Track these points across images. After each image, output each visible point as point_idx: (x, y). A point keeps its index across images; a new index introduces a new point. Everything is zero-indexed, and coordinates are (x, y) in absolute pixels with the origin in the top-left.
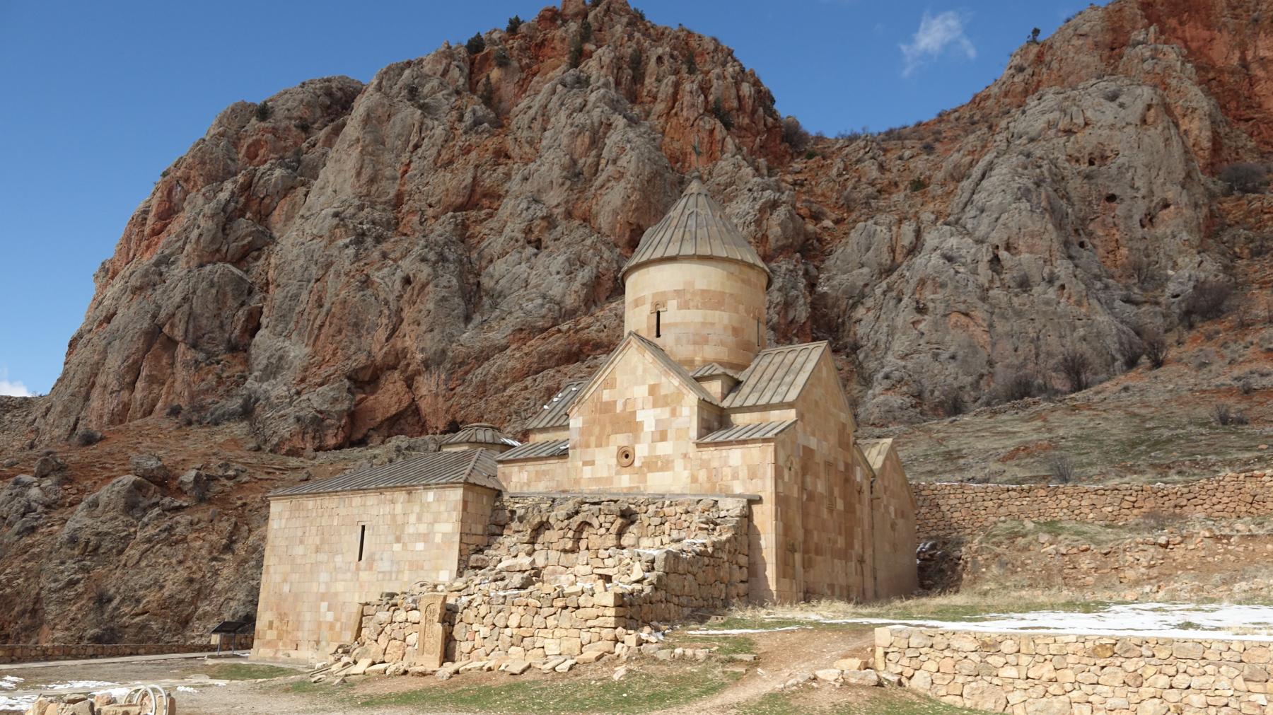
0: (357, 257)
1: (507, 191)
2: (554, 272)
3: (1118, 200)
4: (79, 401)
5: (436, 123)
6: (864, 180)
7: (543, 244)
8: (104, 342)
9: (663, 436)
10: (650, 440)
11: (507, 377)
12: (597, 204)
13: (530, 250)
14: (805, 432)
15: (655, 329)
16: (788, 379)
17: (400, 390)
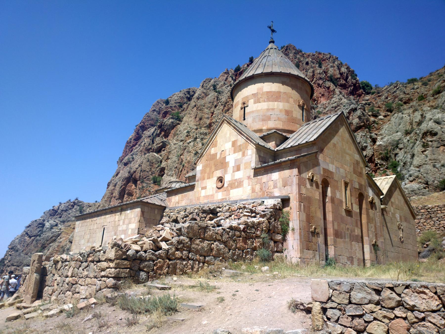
0: (194, 146)
4: (108, 202)
5: (222, 97)
9: (238, 168)
15: (243, 116)
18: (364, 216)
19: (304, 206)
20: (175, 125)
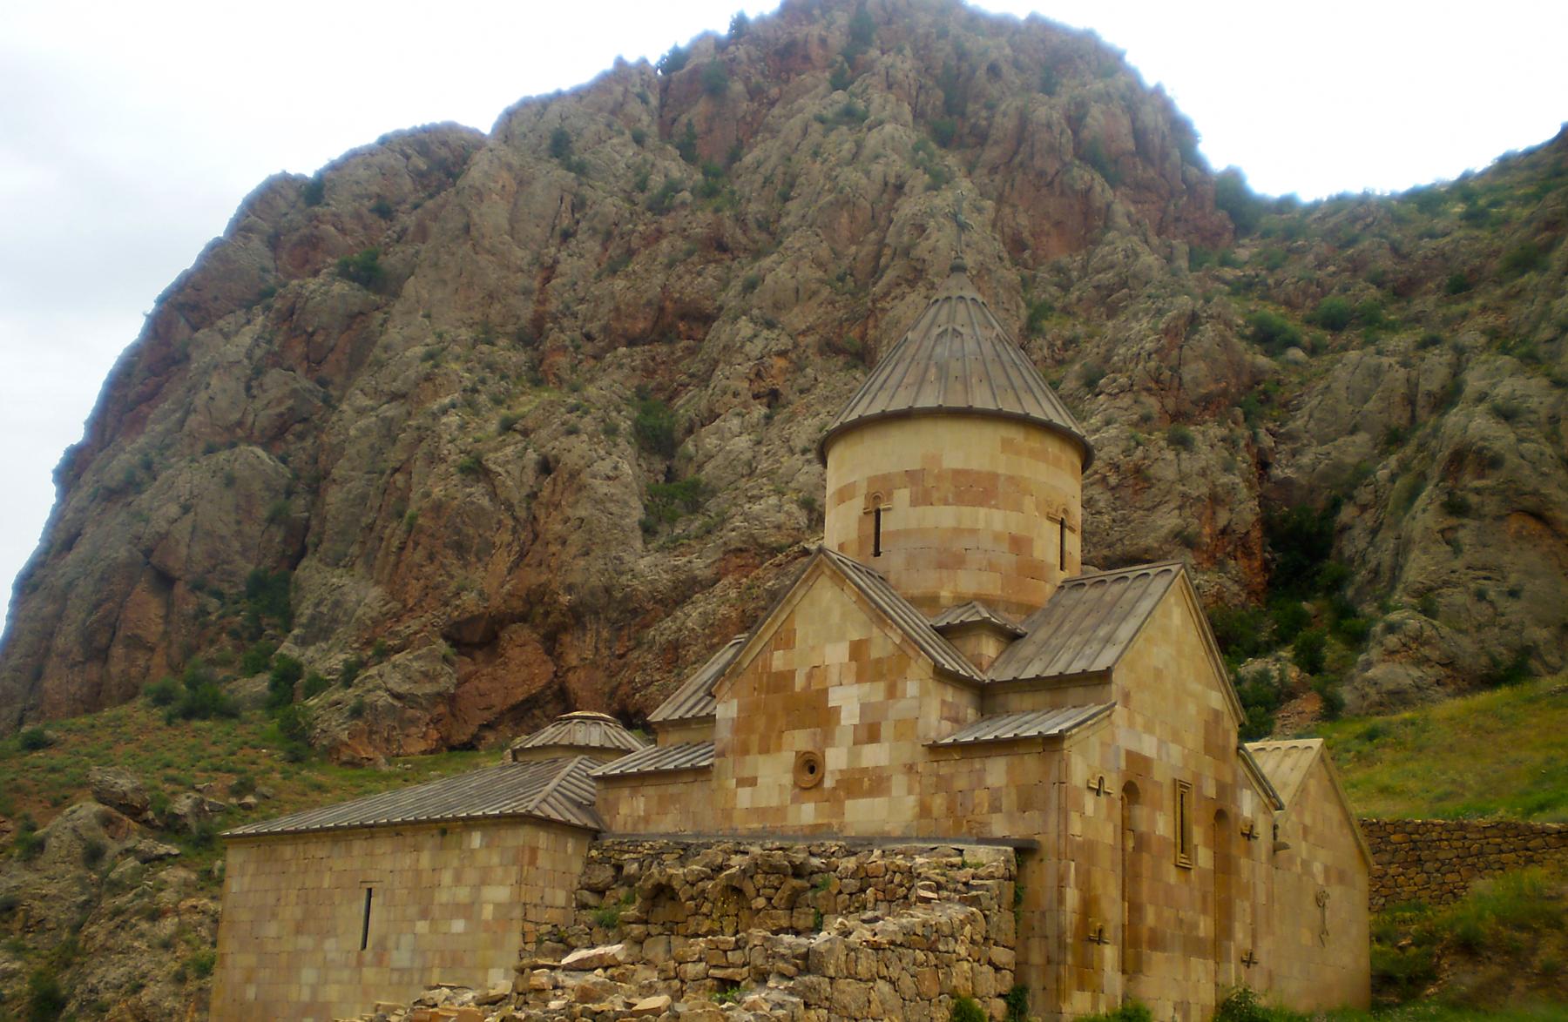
1: (721, 308)
7: (782, 401)
9: (870, 733)
10: (850, 738)
11: (713, 635)
12: (876, 327)
13: (759, 410)
14: (1131, 725)
15: (872, 542)
16: (1102, 632)
19: (1076, 870)
20: (356, 309)
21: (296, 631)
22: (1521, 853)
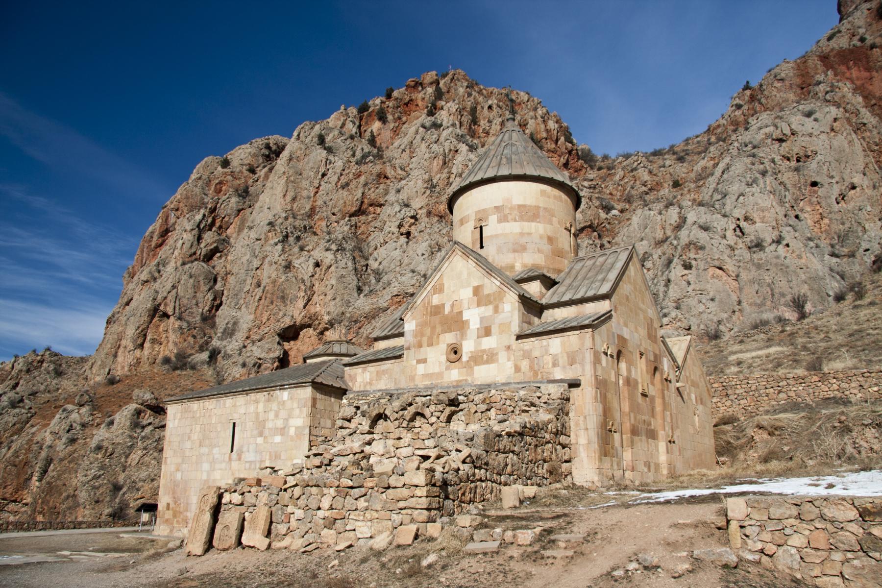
1: (386, 201)
2: (420, 254)
3: (819, 186)
4: (111, 358)
6: (638, 182)
8: (125, 318)
9: (487, 332)
13: (403, 239)
16: (600, 277)
17: (314, 342)
18: (658, 402)
19: (600, 393)
20: (241, 207)
21: (219, 335)
22: (775, 388)
